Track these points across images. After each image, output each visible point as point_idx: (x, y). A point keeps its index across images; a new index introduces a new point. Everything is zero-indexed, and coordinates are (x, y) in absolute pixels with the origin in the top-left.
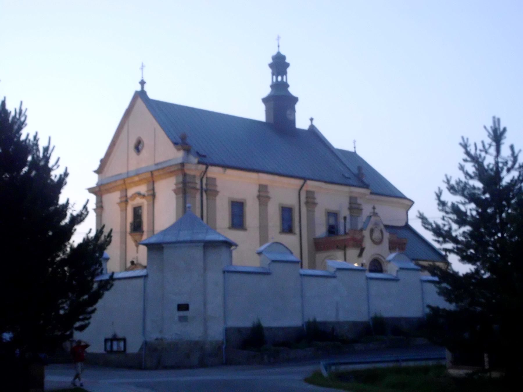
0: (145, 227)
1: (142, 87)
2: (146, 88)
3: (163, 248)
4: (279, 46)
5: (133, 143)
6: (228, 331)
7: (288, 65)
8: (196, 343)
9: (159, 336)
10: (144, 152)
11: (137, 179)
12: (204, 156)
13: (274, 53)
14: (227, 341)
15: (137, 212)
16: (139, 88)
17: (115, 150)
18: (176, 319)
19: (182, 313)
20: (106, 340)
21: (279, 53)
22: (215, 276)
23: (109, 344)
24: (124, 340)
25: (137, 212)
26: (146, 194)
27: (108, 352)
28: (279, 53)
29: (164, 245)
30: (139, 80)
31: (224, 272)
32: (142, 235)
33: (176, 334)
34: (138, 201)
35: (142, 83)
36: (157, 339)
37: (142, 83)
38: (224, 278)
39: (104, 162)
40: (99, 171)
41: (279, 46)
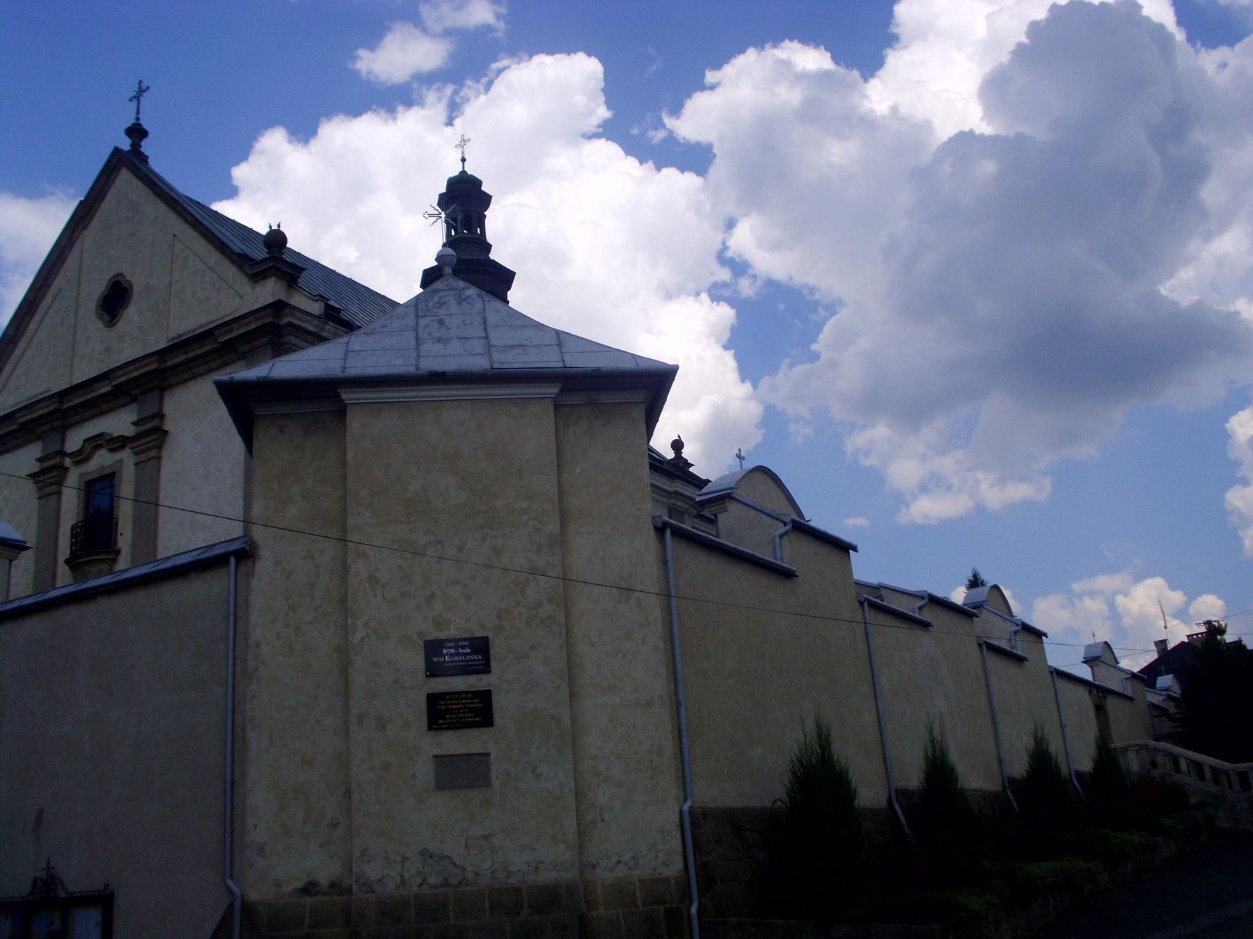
0: (125, 539)
1: (136, 146)
2: (147, 147)
3: (341, 412)
4: (463, 160)
5: (97, 287)
7: (486, 200)
9: (323, 868)
10: (132, 314)
11: (105, 389)
12: (338, 310)
13: (455, 171)
14: (707, 878)
15: (100, 491)
16: (125, 144)
17: (32, 326)
18: (425, 771)
19: (453, 742)
21: (463, 173)
22: (620, 544)
24: (104, 901)
25: (100, 491)
26: (130, 431)
28: (463, 173)
29: (347, 396)
30: (130, 121)
31: (660, 530)
32: (115, 560)
33: (426, 854)
34: (102, 460)
35: (137, 132)
36: (309, 889)
37: (137, 132)
38: (664, 563)
41: (463, 160)
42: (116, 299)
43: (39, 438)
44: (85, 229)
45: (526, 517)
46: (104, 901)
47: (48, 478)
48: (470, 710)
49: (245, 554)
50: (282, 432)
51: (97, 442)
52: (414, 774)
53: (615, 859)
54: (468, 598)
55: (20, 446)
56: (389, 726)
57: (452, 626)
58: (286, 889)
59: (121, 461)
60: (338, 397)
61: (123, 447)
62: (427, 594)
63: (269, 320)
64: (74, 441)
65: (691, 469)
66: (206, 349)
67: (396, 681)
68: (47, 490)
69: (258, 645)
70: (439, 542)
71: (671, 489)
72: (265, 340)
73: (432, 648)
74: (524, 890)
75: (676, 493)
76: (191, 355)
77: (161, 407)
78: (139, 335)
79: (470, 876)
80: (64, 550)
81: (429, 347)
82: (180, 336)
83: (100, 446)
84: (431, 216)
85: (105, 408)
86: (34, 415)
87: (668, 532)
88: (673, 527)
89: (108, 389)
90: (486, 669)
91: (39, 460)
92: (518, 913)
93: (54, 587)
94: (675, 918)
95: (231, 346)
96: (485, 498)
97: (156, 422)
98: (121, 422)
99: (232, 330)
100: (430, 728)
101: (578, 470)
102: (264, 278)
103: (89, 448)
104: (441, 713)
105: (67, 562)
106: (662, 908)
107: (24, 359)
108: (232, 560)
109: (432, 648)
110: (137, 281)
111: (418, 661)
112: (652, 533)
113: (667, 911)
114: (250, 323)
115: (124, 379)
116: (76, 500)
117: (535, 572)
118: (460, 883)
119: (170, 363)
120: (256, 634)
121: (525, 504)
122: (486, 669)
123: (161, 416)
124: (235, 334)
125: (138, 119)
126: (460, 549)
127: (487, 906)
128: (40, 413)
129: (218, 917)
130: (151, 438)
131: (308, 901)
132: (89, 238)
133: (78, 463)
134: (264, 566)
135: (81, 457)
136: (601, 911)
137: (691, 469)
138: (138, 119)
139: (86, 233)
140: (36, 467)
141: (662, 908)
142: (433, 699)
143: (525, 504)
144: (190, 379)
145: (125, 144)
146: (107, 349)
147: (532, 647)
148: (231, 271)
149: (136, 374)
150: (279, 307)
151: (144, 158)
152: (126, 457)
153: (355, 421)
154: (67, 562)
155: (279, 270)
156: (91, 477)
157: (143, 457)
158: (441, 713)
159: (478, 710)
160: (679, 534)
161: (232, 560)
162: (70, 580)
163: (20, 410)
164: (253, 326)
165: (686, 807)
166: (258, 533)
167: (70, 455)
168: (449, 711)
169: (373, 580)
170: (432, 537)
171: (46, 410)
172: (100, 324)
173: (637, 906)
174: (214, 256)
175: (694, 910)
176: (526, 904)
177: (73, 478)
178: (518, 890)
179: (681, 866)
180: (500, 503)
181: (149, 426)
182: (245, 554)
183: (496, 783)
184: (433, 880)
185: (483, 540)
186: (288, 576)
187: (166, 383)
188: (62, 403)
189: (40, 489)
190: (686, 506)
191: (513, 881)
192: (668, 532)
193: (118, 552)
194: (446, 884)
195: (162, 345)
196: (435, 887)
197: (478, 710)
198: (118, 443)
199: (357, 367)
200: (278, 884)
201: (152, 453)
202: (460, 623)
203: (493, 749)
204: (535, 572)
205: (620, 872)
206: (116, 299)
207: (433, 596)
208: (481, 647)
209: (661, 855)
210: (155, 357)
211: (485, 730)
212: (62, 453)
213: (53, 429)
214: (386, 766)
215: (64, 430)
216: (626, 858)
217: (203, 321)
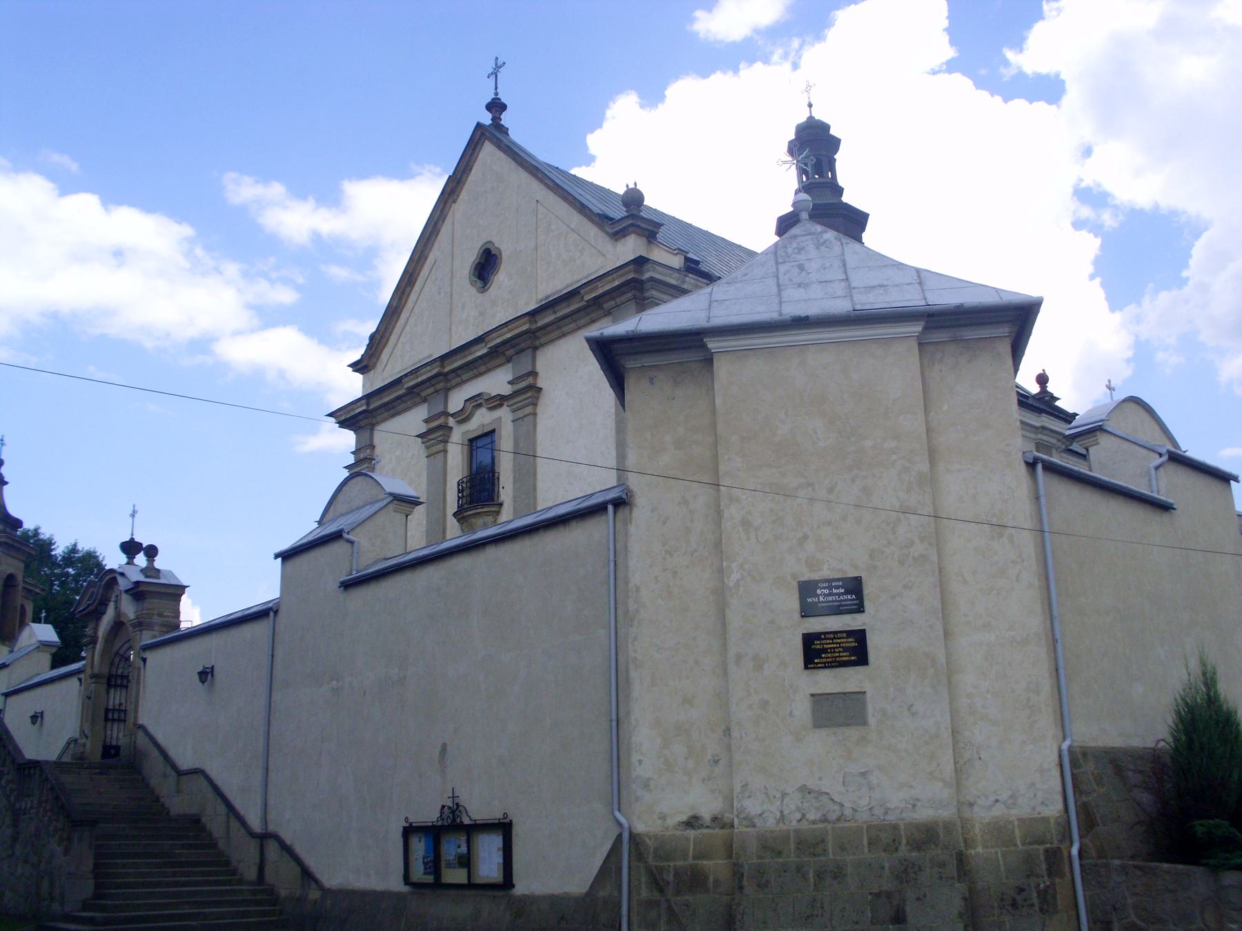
0: (506, 493)
1: (496, 120)
2: (506, 119)
3: (709, 361)
4: (810, 105)
5: (470, 257)
6: (1077, 764)
7: (835, 144)
8: (926, 836)
9: (708, 806)
10: (502, 278)
11: (481, 351)
12: (697, 263)
13: (802, 119)
14: (1088, 820)
16: (487, 119)
17: (413, 297)
18: (802, 709)
19: (829, 681)
20: (409, 831)
21: (811, 118)
22: (991, 479)
23: (419, 847)
26: (506, 390)
27: (417, 886)
28: (811, 118)
29: (713, 344)
31: (1031, 465)
32: (498, 513)
33: (805, 790)
34: (482, 419)
35: (496, 107)
36: (692, 822)
37: (496, 107)
39: (377, 343)
40: (360, 367)
41: (810, 105)
42: (486, 266)
43: (425, 400)
44: (454, 202)
45: (894, 457)
46: (504, 828)
47: (435, 435)
48: (845, 650)
49: (621, 503)
50: (652, 383)
51: (477, 401)
52: (791, 714)
53: (992, 799)
54: (840, 538)
55: (409, 409)
56: (766, 666)
57: (825, 567)
58: (671, 822)
59: (500, 418)
60: (704, 346)
61: (501, 405)
62: (800, 535)
63: (631, 276)
64: (456, 401)
65: (1057, 403)
66: (573, 308)
67: (772, 622)
68: (434, 449)
69: (638, 589)
70: (811, 485)
71: (1038, 425)
72: (629, 295)
73: (806, 589)
74: (902, 826)
75: (1043, 428)
76: (560, 314)
77: (534, 364)
78: (510, 299)
79: (848, 812)
80: (452, 505)
81: (791, 293)
82: (548, 297)
83: (480, 405)
84: (785, 162)
85: (482, 369)
86: (420, 379)
87: (1039, 466)
88: (1043, 461)
89: (485, 351)
90: (860, 609)
91: (426, 421)
92: (896, 849)
93: (444, 540)
94: (1055, 859)
95: (597, 302)
96: (853, 439)
97: (530, 380)
98: (497, 382)
99: (596, 288)
100: (806, 668)
101: (945, 408)
102: (625, 236)
103: (470, 406)
104: (815, 652)
105: (455, 515)
106: (1042, 848)
107: (408, 328)
108: (610, 508)
109: (806, 589)
110: (505, 247)
111: (792, 602)
112: (1023, 469)
113: (1047, 851)
114: (614, 280)
115: (499, 340)
116: (460, 457)
117: (905, 511)
118: (838, 819)
119: (540, 324)
120: (635, 579)
121: (893, 444)
122: (860, 609)
123: (534, 374)
124: (600, 291)
125: (496, 94)
126: (831, 490)
127: (865, 842)
128: (424, 377)
129: (607, 846)
130: (527, 393)
131: (692, 833)
132: (458, 209)
133: (460, 422)
134: (641, 512)
135: (463, 417)
136: (980, 849)
137: (1057, 403)
138: (496, 94)
139: (454, 206)
140: (423, 428)
141: (1042, 848)
142: (809, 640)
143: (893, 444)
144: (559, 338)
145: (487, 119)
146: (481, 314)
147: (905, 587)
148: (592, 231)
149: (509, 335)
150: (640, 262)
151: (505, 131)
152: (504, 413)
153: (722, 368)
154: (455, 515)
155: (638, 226)
156: (472, 436)
157: (520, 414)
158: (815, 652)
159: (856, 650)
160: (1050, 468)
161: (610, 508)
162: (459, 533)
163: (406, 375)
164: (617, 283)
165: (1065, 746)
166: (633, 481)
167: (452, 415)
168: (825, 651)
169: (746, 524)
170: (803, 480)
171: (429, 375)
172: (473, 290)
173: (1016, 845)
174: (576, 219)
175: (1075, 851)
176: (904, 841)
177: (459, 435)
178: (895, 827)
179: (1060, 806)
180: (868, 443)
181: (523, 384)
182: (621, 503)
183: (872, 720)
184: (812, 816)
185: (853, 480)
186: (664, 523)
187: (537, 343)
188: (443, 366)
189: (427, 448)
190: (1054, 441)
191: (891, 818)
192: (1039, 466)
193: (501, 505)
194: (825, 820)
195: (532, 307)
196: (814, 822)
197: (856, 650)
198: (498, 401)
199: (721, 317)
200: (663, 817)
201: (528, 410)
202: (835, 564)
203: (868, 688)
204: (905, 511)
205: (998, 811)
206: (486, 266)
207: (806, 537)
208: (855, 587)
209: (1040, 795)
210: (527, 318)
211: (860, 669)
212: (446, 414)
213: (437, 391)
214: (765, 704)
215: (447, 391)
216: (1004, 796)
217: (569, 281)
